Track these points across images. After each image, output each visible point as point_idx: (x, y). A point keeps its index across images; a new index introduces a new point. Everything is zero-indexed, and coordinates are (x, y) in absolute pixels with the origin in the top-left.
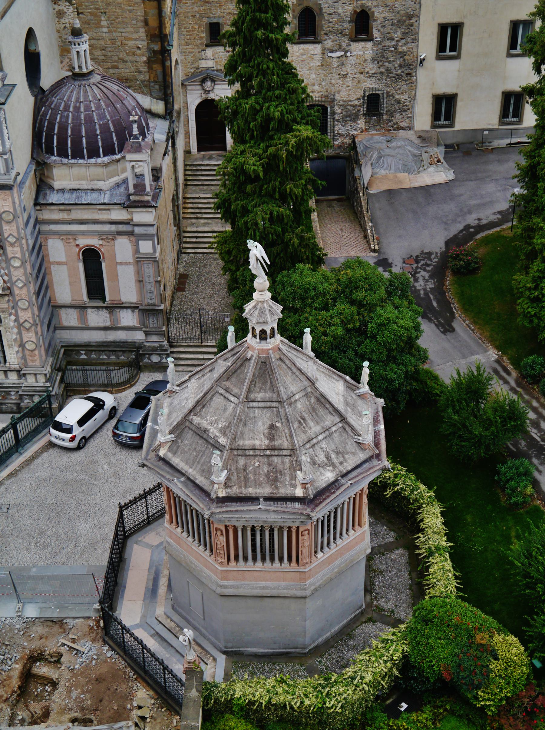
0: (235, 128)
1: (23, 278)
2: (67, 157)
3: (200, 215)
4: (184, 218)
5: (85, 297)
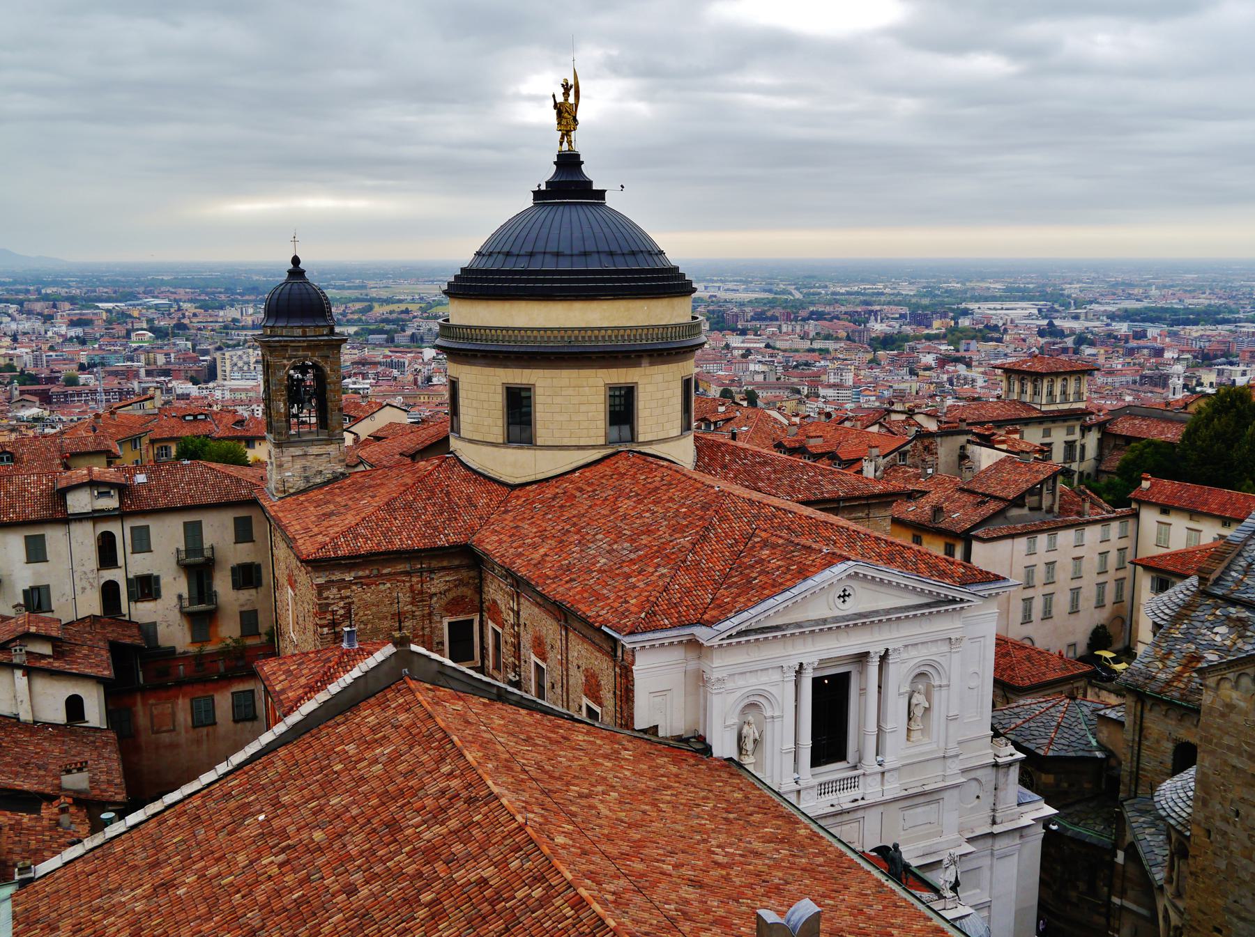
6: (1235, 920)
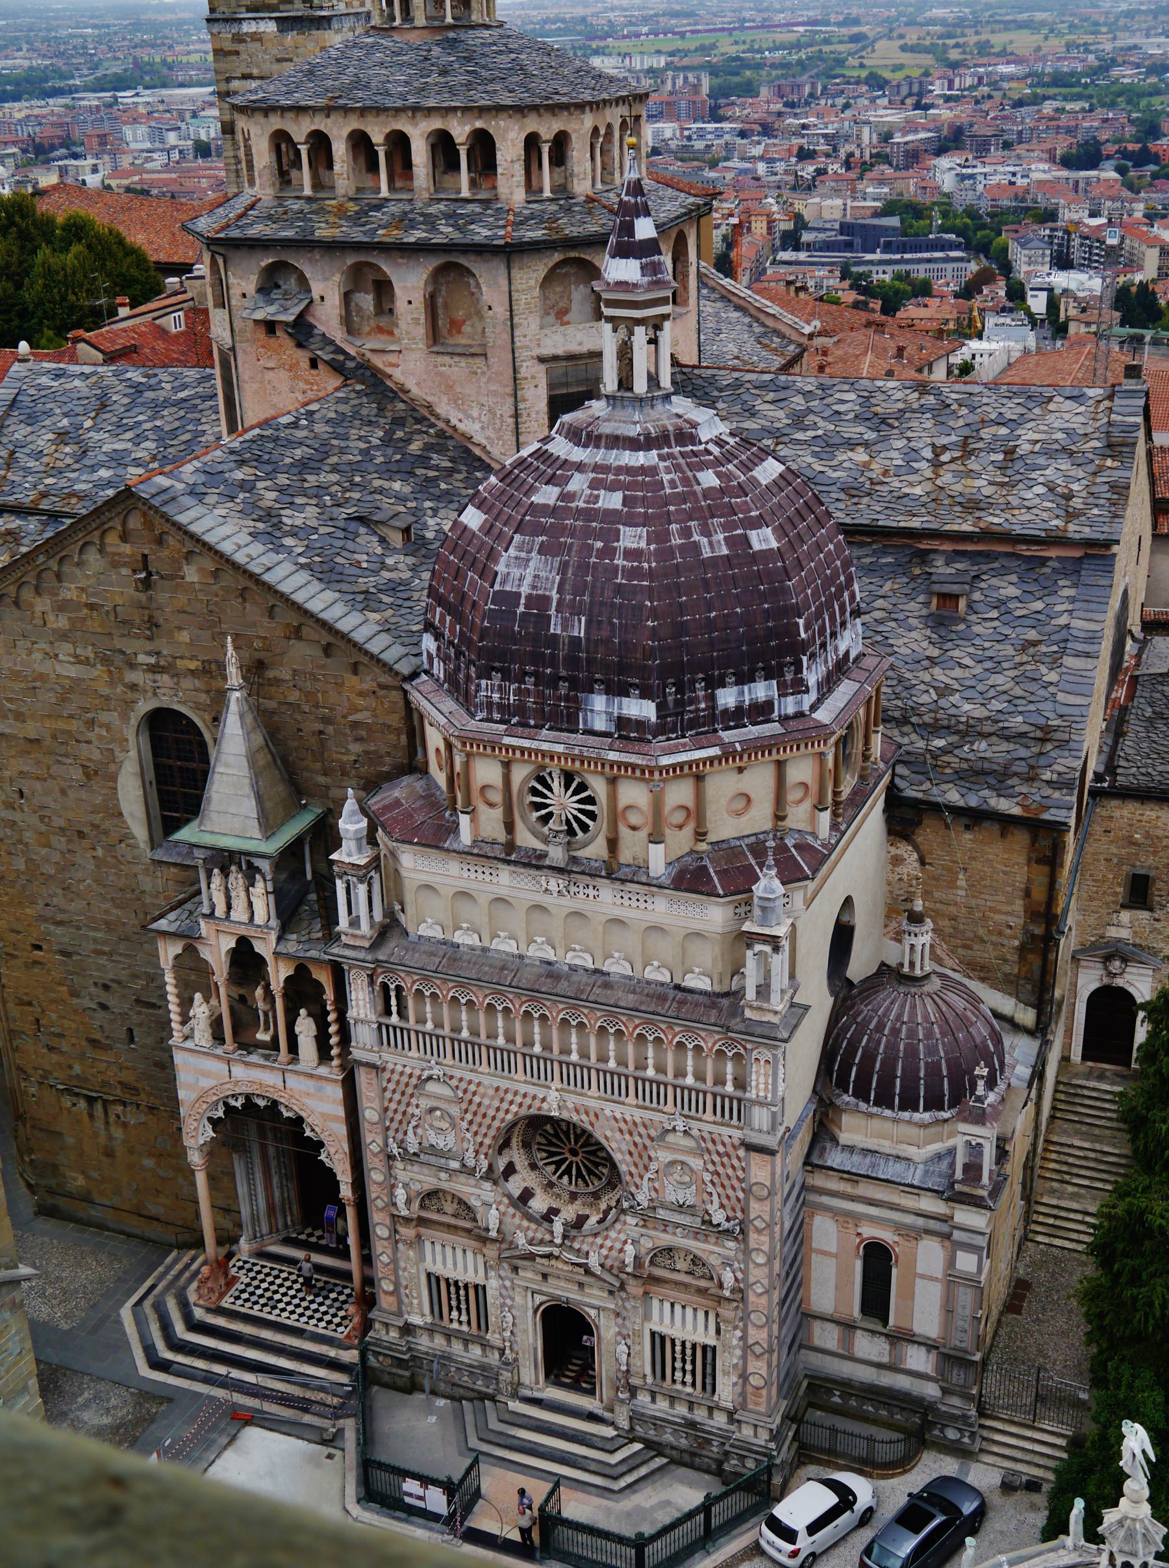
0: (1141, 1143)
1: (766, 1282)
2: (867, 1101)
3: (1067, 1177)
4: (1040, 1176)
5: (856, 1312)
6: (52, 928)
